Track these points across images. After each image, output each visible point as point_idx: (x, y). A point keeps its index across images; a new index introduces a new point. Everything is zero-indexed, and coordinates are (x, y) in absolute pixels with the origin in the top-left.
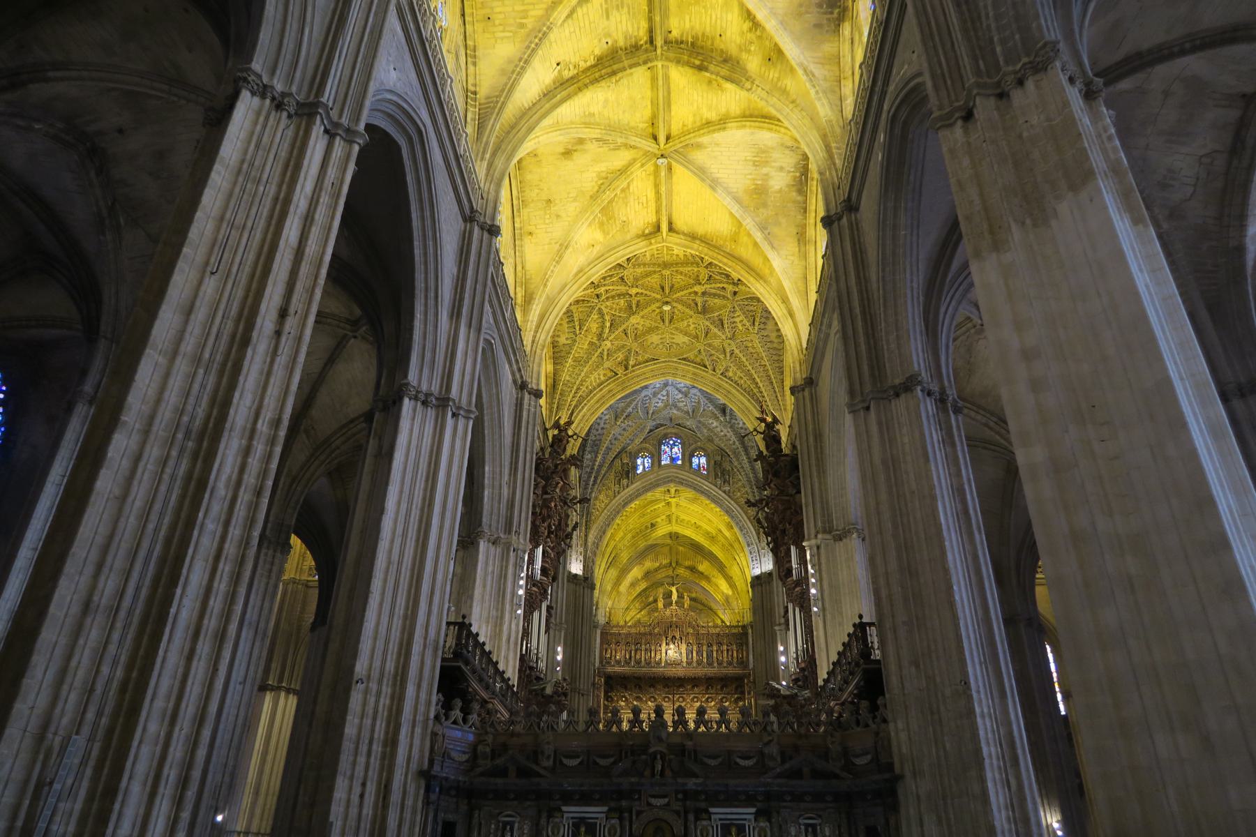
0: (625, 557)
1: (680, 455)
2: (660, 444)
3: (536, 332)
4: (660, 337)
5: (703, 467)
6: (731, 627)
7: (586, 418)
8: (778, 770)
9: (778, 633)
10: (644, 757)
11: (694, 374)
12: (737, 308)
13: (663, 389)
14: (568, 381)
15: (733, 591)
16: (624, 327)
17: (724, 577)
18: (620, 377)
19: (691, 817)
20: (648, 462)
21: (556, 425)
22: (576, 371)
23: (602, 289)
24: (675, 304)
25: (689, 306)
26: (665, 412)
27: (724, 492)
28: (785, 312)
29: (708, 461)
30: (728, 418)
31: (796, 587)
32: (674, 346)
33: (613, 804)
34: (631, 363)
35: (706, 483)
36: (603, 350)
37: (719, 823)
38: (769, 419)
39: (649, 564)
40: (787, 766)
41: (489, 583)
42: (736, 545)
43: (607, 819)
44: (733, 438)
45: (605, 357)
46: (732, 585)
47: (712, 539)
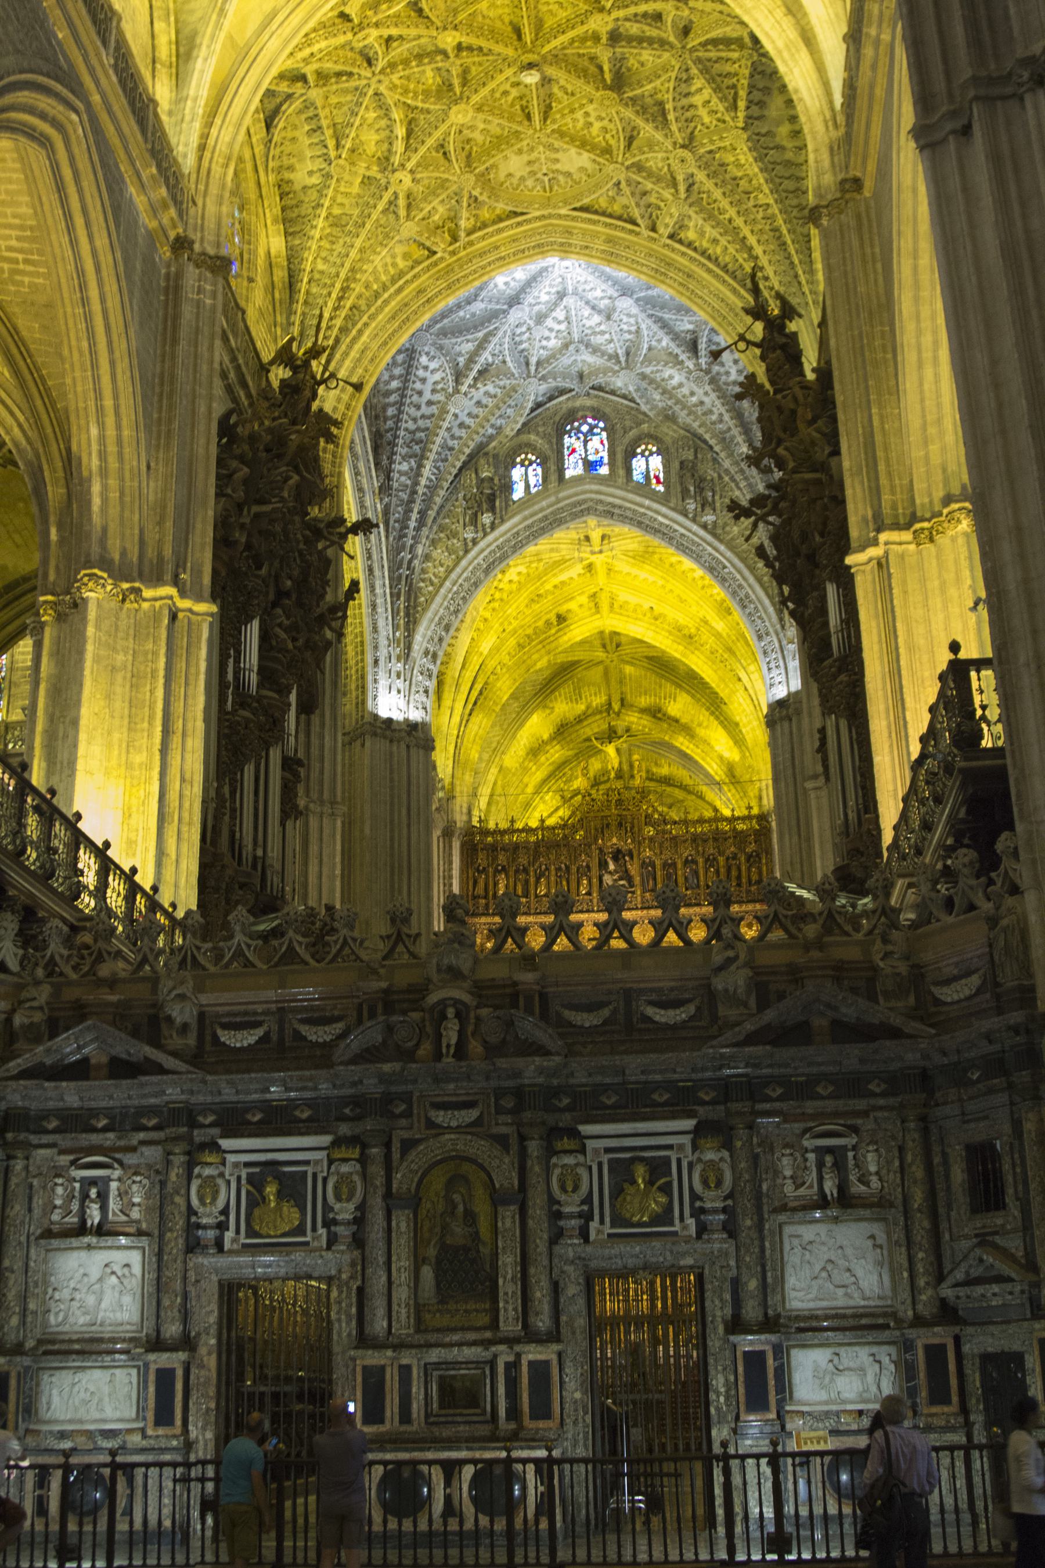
0: (504, 688)
1: (605, 455)
2: (560, 433)
3: (209, 125)
4: (525, 158)
5: (657, 478)
6: (732, 820)
7: (369, 355)
8: (749, 1027)
9: (813, 795)
10: (416, 1016)
11: (609, 240)
12: (694, 71)
13: (556, 305)
14: (322, 272)
15: (742, 752)
16: (438, 134)
17: (721, 723)
18: (442, 259)
19: (534, 1147)
20: (535, 474)
21: (285, 356)
22: (338, 248)
23: (372, 36)
24: (551, 71)
25: (583, 74)
26: (565, 361)
27: (704, 527)
28: (793, 35)
29: (666, 465)
30: (703, 361)
31: (840, 671)
32: (561, 178)
33: (344, 1129)
34: (463, 223)
35: (664, 510)
36: (396, 195)
37: (605, 1158)
38: (774, 309)
39: (563, 708)
40: (769, 1016)
41: (119, 690)
42: (740, 648)
43: (331, 1162)
44: (719, 408)
45: (402, 213)
46: (739, 741)
47: (689, 639)
